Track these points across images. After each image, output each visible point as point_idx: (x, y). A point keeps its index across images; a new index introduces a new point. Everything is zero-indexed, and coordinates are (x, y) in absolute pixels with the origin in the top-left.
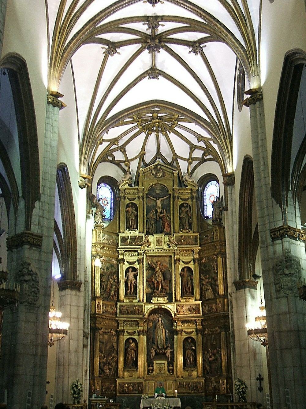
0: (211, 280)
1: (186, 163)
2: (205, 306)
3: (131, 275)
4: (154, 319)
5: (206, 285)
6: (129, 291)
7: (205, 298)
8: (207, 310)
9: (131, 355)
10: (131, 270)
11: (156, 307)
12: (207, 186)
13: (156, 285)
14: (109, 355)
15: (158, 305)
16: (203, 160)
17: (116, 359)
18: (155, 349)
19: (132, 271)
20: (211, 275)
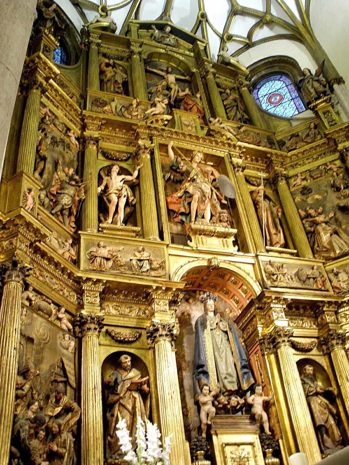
0: (335, 214)
1: (218, 41)
2: (336, 275)
3: (116, 181)
4: (183, 314)
5: (326, 223)
6: (110, 220)
7: (335, 251)
8: (344, 282)
9: (130, 408)
10: (115, 169)
11: (205, 263)
12: (258, 87)
13: (194, 206)
14: (48, 397)
15: (210, 257)
16: (248, 45)
17: (76, 419)
18: (213, 393)
19: (119, 174)
20: (329, 205)
